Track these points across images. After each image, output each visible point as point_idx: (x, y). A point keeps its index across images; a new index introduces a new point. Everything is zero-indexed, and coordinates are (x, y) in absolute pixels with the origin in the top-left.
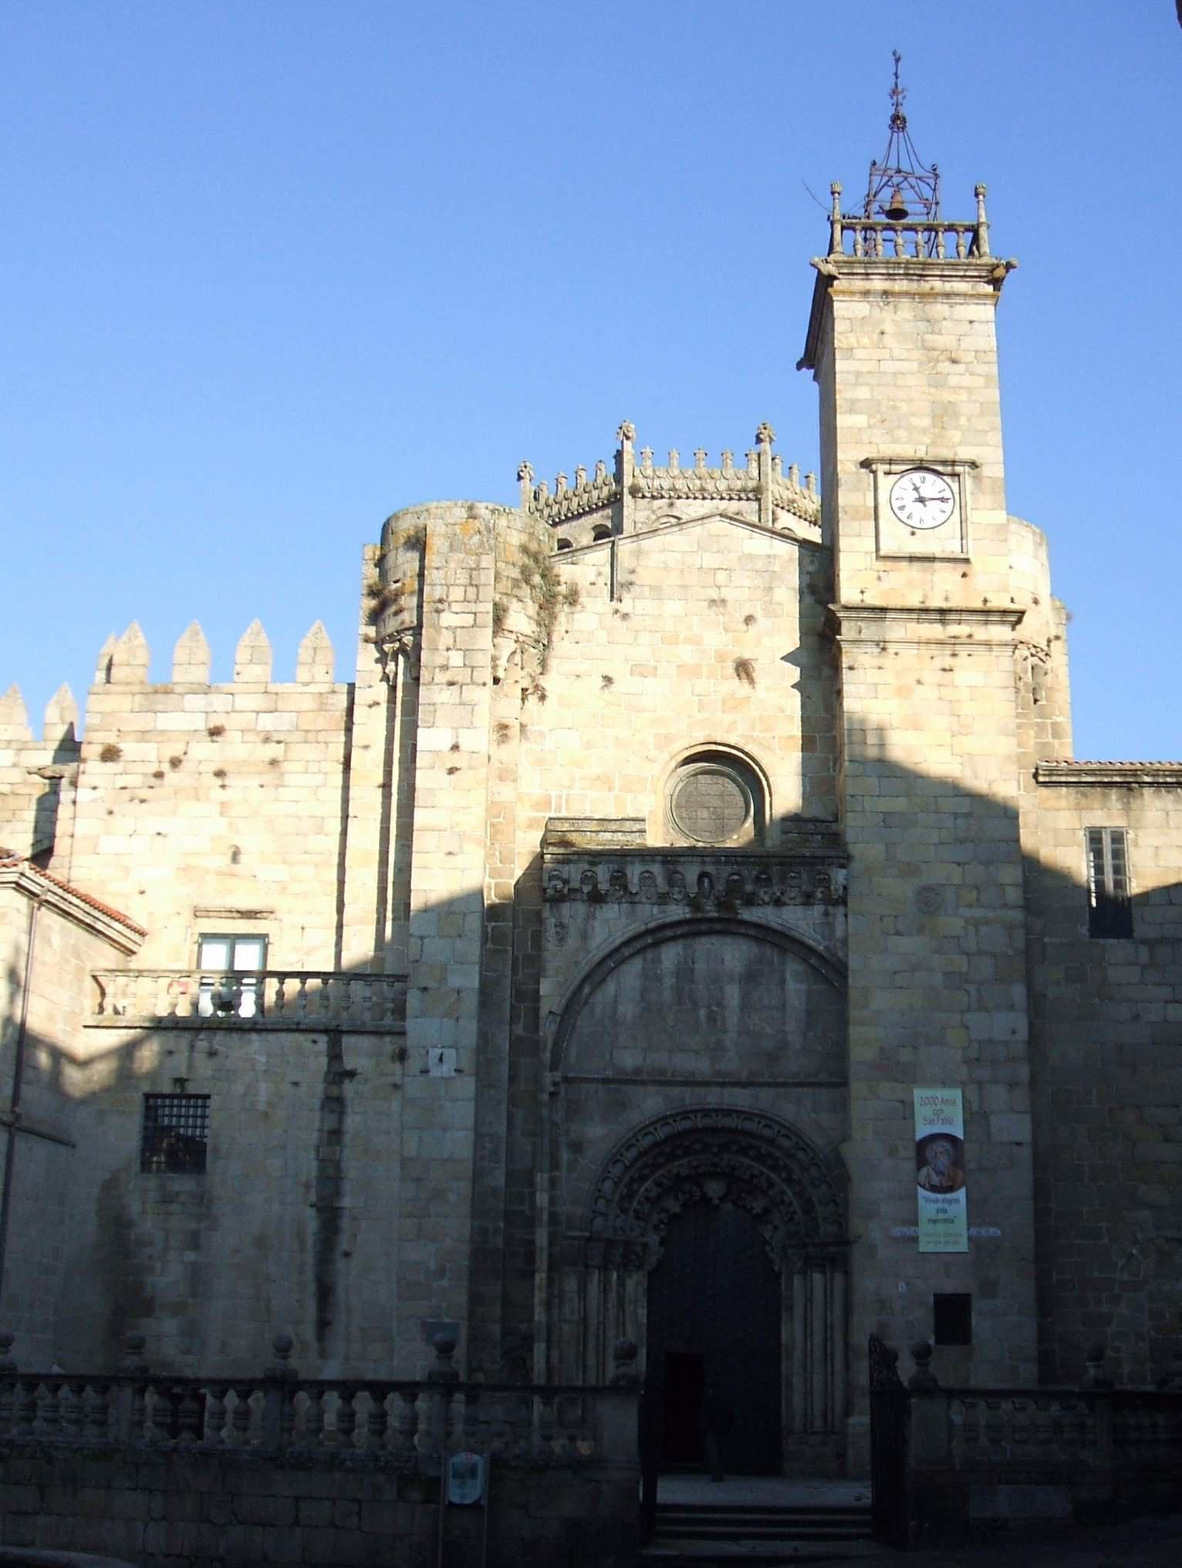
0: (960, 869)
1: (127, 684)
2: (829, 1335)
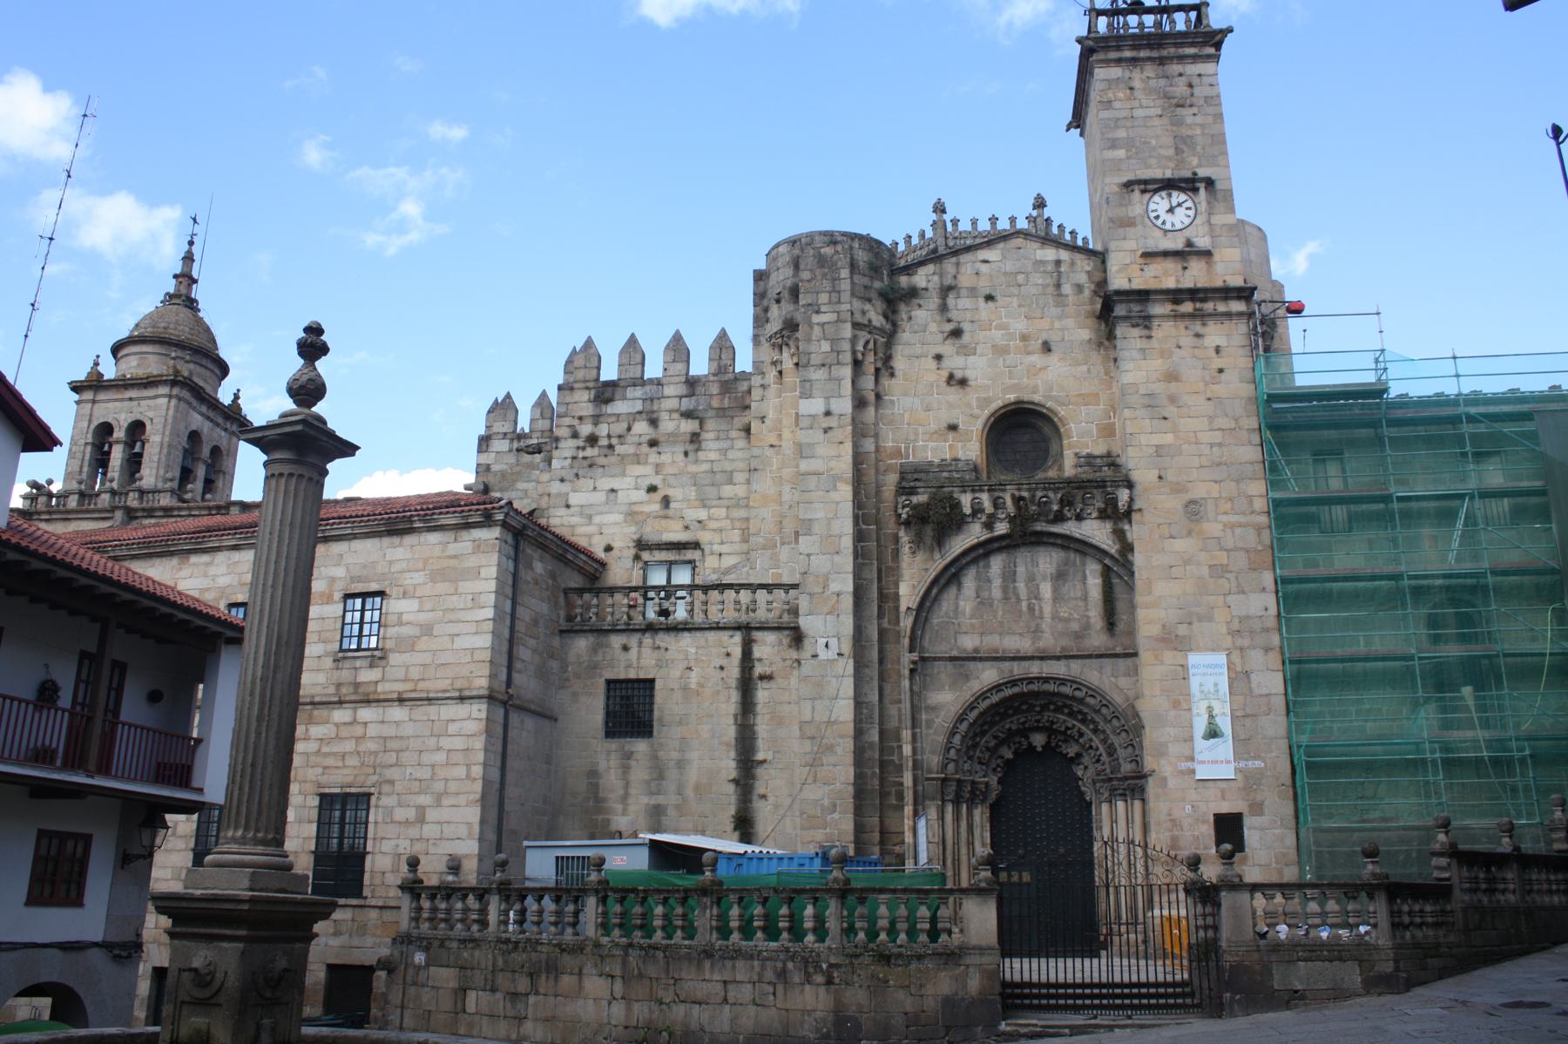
0: (1217, 486)
1: (586, 381)
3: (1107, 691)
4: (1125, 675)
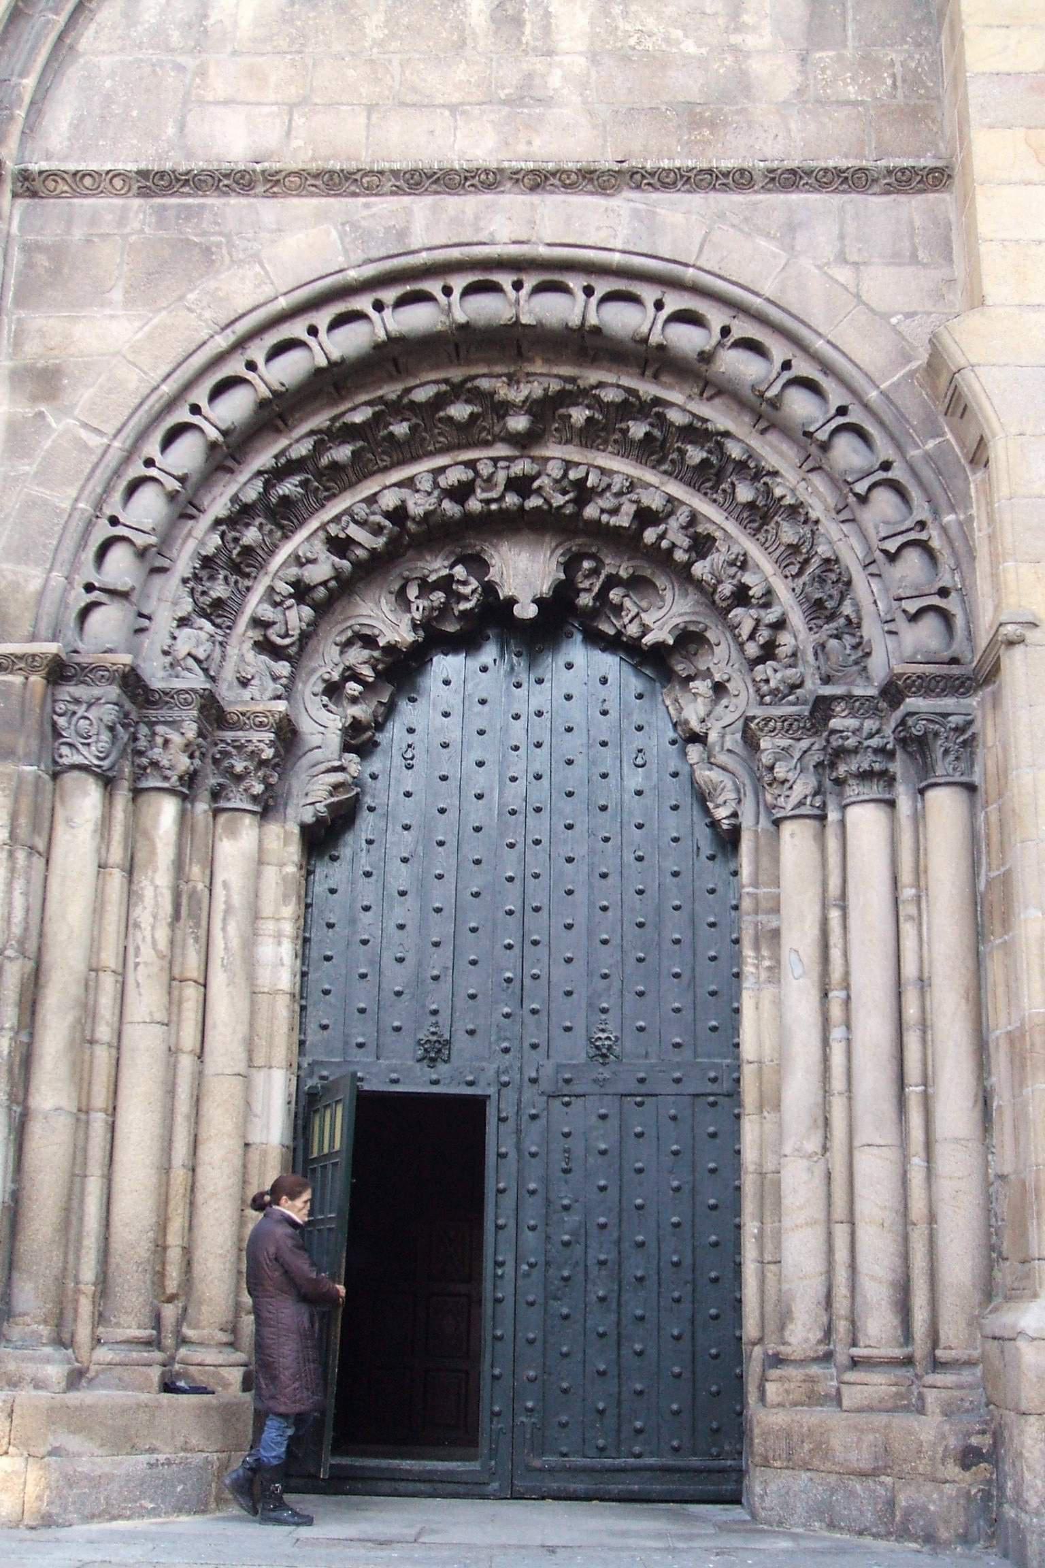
2: (912, 1011)
3: (817, 318)
4: (895, 259)
